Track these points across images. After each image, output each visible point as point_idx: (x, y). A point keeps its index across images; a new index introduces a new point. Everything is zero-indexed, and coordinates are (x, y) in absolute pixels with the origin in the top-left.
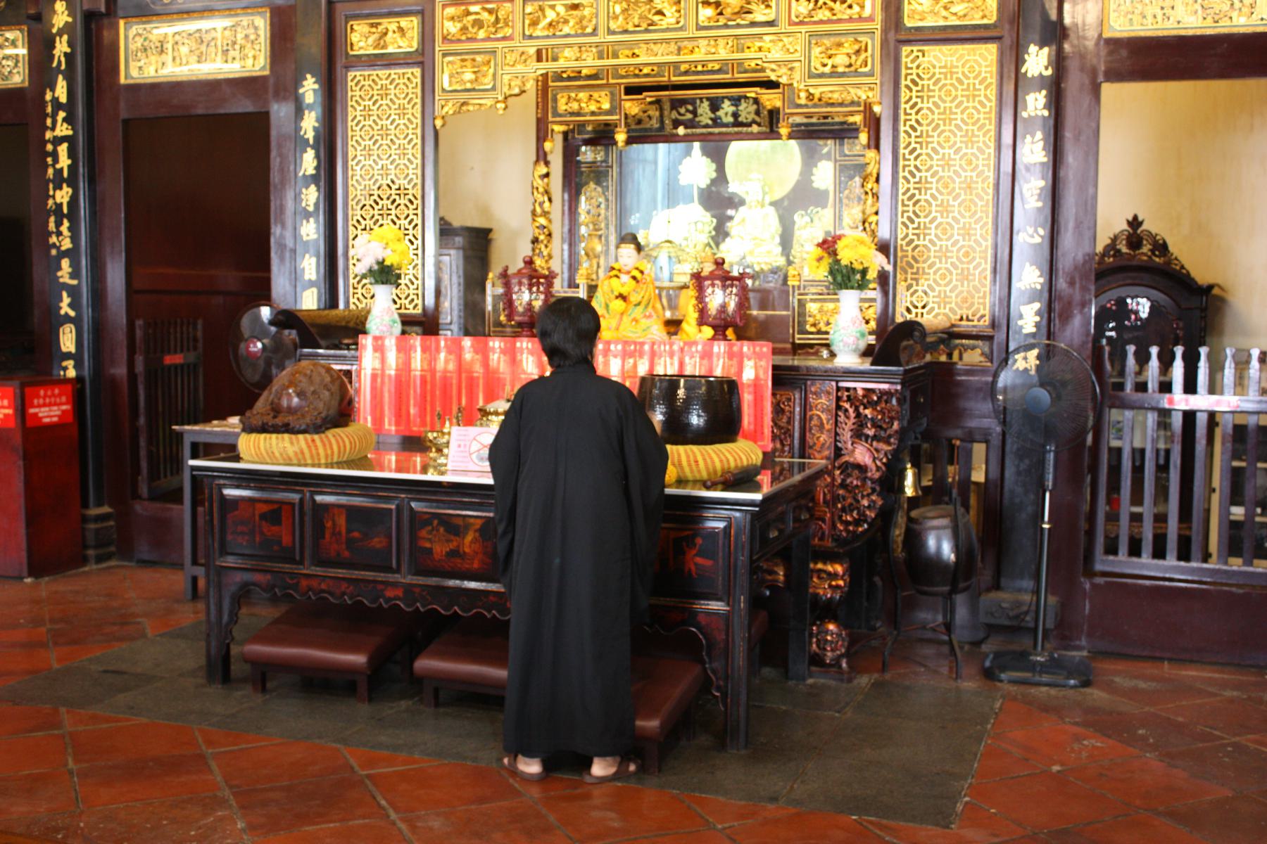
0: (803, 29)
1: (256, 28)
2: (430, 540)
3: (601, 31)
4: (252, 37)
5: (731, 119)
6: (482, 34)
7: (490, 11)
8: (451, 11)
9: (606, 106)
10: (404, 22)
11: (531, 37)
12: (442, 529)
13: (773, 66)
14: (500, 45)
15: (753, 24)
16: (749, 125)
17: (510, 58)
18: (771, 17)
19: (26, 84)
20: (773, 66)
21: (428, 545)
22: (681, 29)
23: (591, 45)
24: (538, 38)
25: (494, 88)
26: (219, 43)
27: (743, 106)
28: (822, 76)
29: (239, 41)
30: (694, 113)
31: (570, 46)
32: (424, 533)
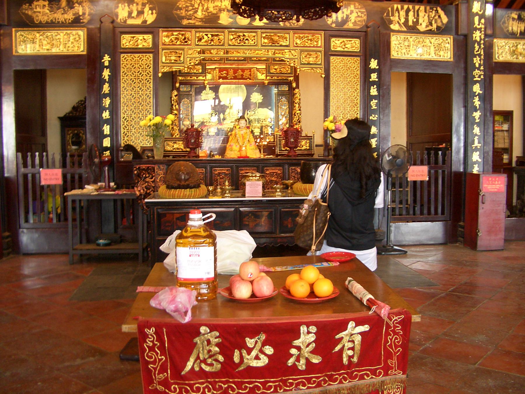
0: (299, 48)
1: (79, 35)
2: (249, 222)
3: (226, 44)
4: (77, 39)
5: (241, 77)
6: (178, 43)
7: (183, 35)
8: (165, 34)
9: (200, 71)
10: (146, 36)
11: (198, 45)
12: (253, 217)
13: (288, 60)
14: (186, 47)
15: (281, 46)
16: (246, 79)
17: (190, 52)
18: (288, 44)
19: (392, 57)
20: (288, 60)
21: (247, 223)
22: (255, 46)
23: (222, 49)
24: (201, 45)
25: (183, 63)
26: (61, 40)
27: (246, 72)
28: (304, 64)
29: (71, 40)
30: (227, 74)
31: (214, 49)
32: (246, 219)
